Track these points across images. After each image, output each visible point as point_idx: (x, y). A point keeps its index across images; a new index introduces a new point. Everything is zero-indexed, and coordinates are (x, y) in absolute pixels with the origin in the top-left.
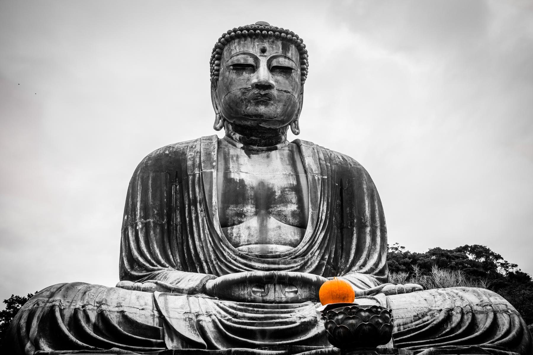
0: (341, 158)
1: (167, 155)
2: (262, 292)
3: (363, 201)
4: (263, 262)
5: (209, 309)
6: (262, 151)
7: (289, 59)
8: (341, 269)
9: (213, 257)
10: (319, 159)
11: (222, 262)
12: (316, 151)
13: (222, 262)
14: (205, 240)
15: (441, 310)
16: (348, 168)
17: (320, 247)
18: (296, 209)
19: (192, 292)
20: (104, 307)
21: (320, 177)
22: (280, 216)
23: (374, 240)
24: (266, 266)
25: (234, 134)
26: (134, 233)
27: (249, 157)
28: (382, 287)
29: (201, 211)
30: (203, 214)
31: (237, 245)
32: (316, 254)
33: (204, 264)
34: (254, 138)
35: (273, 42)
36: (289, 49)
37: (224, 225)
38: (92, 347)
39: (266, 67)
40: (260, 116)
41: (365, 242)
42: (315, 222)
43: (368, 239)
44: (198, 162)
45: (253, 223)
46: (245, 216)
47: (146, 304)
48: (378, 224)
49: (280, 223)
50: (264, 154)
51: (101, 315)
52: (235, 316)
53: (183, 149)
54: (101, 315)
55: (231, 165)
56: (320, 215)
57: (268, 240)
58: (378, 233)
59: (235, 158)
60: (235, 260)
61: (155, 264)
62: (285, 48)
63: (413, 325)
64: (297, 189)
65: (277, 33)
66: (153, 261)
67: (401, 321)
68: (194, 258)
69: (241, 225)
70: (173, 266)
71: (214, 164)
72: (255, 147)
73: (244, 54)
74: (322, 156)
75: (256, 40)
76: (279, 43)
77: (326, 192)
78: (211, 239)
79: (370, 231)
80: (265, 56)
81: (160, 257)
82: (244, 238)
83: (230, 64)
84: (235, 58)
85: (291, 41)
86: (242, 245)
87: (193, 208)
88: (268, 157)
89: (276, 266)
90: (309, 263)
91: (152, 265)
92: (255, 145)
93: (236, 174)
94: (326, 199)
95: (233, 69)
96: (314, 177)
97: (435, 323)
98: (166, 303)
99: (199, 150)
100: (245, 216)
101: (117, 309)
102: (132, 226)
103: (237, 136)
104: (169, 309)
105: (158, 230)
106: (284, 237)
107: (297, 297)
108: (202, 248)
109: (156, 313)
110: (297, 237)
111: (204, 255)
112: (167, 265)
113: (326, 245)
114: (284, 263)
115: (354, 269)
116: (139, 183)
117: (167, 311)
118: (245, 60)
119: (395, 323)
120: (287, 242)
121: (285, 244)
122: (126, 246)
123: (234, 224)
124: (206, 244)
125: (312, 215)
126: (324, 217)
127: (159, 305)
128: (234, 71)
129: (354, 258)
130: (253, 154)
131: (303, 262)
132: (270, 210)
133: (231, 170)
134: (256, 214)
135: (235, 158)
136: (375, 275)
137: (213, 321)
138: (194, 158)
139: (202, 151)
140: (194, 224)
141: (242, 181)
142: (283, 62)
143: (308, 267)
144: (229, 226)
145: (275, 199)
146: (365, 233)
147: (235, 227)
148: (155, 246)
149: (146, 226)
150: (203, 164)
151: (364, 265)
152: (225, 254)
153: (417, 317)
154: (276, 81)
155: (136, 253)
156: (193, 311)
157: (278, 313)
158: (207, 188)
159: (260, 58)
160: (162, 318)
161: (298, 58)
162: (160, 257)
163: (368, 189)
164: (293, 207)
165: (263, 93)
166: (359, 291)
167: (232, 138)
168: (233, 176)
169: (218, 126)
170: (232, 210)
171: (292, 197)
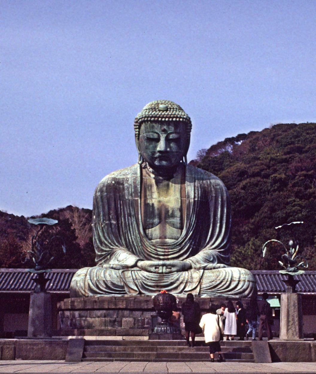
1: (114, 184)
3: (218, 209)
4: (162, 248)
9: (140, 245)
11: (144, 247)
13: (144, 247)
14: (136, 236)
15: (220, 279)
16: (211, 189)
20: (104, 279)
24: (163, 250)
25: (149, 168)
26: (101, 228)
29: (134, 221)
30: (135, 222)
33: (136, 247)
38: (104, 293)
39: (164, 141)
41: (216, 232)
44: (130, 193)
47: (118, 277)
48: (224, 221)
51: (104, 281)
52: (148, 279)
53: (122, 180)
54: (104, 281)
55: (148, 193)
56: (191, 222)
59: (150, 187)
60: (150, 247)
61: (113, 245)
63: (208, 285)
66: (112, 244)
67: (205, 283)
68: (131, 243)
69: (152, 229)
73: (152, 132)
78: (139, 236)
83: (145, 136)
86: (153, 239)
87: (129, 218)
88: (168, 186)
91: (112, 245)
94: (195, 213)
96: (189, 200)
97: (215, 285)
98: (124, 275)
99: (130, 183)
100: (155, 225)
102: (99, 224)
103: (151, 170)
104: (126, 278)
108: (135, 239)
109: (121, 280)
110: (179, 235)
111: (136, 243)
112: (119, 246)
114: (172, 249)
115: (208, 246)
116: (101, 201)
117: (125, 279)
118: (153, 136)
119: (203, 283)
120: (174, 237)
121: (172, 239)
122: (97, 233)
123: (149, 228)
124: (137, 239)
126: (193, 224)
128: (148, 141)
131: (180, 248)
132: (167, 220)
133: (148, 197)
134: (159, 223)
135: (150, 187)
137: (141, 282)
138: (128, 188)
139: (132, 184)
140: (131, 226)
141: (153, 204)
143: (183, 249)
144: (147, 229)
145: (169, 215)
146: (217, 227)
147: (150, 229)
150: (133, 195)
152: (145, 244)
153: (211, 282)
155: (103, 239)
158: (136, 208)
159: (161, 135)
160: (124, 282)
164: (177, 220)
166: (198, 266)
167: (148, 170)
168: (148, 202)
169: (140, 162)
171: (178, 214)
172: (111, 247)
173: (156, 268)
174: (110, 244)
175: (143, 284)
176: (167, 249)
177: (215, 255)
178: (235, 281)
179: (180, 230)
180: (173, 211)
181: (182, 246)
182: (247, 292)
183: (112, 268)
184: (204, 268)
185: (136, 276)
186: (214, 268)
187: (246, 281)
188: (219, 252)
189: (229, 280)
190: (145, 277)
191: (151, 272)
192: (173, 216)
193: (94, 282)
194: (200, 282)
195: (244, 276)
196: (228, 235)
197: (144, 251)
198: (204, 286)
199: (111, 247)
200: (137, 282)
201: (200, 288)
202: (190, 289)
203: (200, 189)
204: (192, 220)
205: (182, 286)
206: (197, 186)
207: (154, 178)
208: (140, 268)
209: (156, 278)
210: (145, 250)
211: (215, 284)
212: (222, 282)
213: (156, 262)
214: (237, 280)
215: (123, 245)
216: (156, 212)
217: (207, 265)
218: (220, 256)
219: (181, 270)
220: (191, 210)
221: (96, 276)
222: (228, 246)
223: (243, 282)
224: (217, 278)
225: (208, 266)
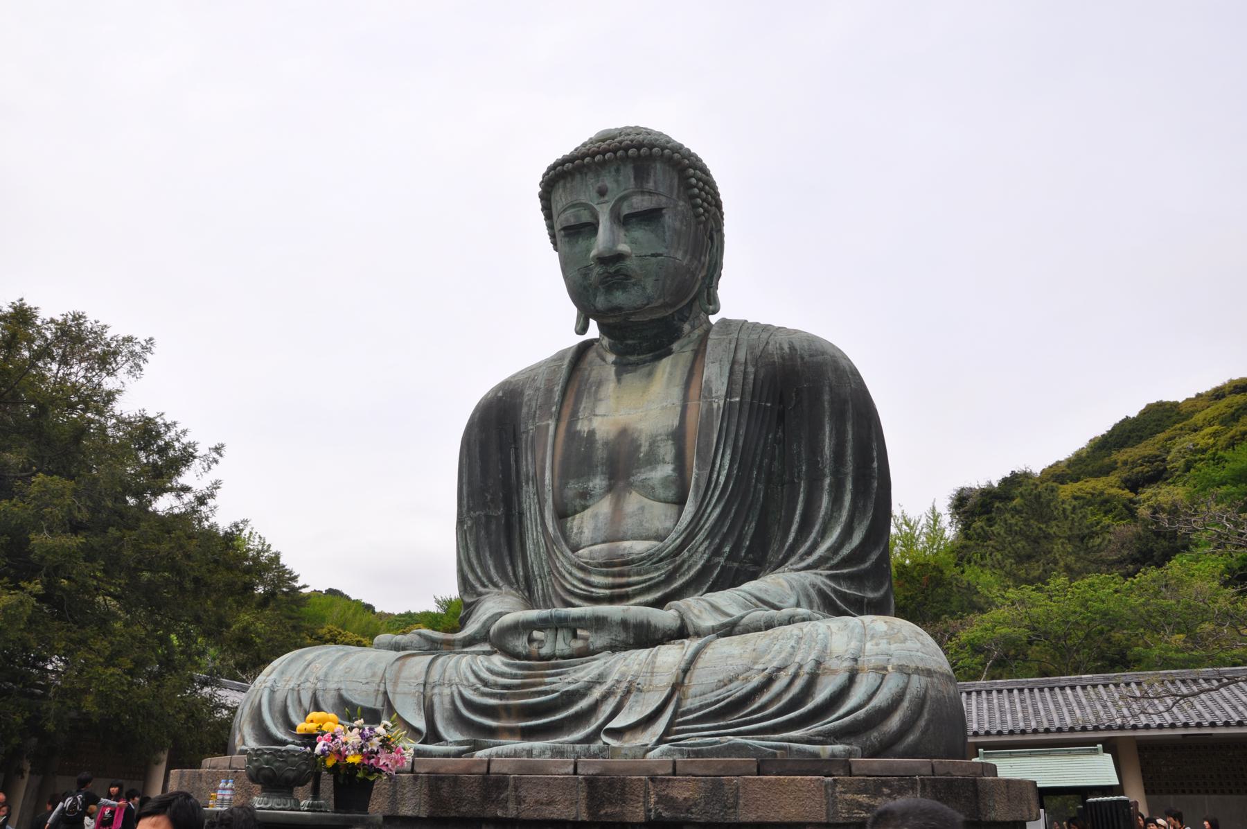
0: (786, 347)
1: (500, 399)
2: (541, 641)
3: (822, 427)
4: (607, 575)
6: (645, 362)
7: (650, 193)
8: (771, 563)
10: (734, 363)
12: (733, 346)
17: (711, 535)
18: (670, 472)
19: (470, 641)
20: (319, 685)
21: (722, 403)
23: (836, 501)
24: (610, 580)
27: (619, 381)
28: (742, 617)
31: (575, 549)
32: (701, 549)
34: (630, 342)
35: (618, 170)
36: (648, 174)
37: (563, 514)
39: (608, 224)
40: (618, 309)
41: (820, 507)
42: (701, 493)
43: (825, 500)
46: (591, 496)
47: (374, 675)
48: (850, 468)
49: (646, 500)
50: (645, 370)
55: (585, 403)
56: (715, 476)
57: (621, 535)
58: (849, 486)
60: (570, 574)
62: (641, 173)
63: (711, 697)
65: (620, 153)
66: (485, 580)
70: (511, 584)
71: (554, 409)
72: (633, 358)
73: (573, 206)
74: (741, 356)
75: (590, 175)
76: (628, 171)
77: (733, 428)
79: (830, 485)
80: (607, 202)
81: (493, 571)
82: (587, 534)
84: (563, 217)
85: (651, 157)
88: (650, 374)
89: (624, 580)
90: (686, 567)
91: (484, 586)
92: (632, 354)
93: (586, 422)
94: (730, 442)
95: (566, 236)
96: (711, 404)
98: (400, 670)
100: (591, 496)
101: (334, 686)
103: (606, 342)
105: (493, 527)
106: (647, 525)
107: (587, 647)
110: (669, 524)
113: (725, 530)
114: (639, 574)
115: (793, 560)
117: (395, 684)
119: (691, 691)
120: (652, 533)
121: (647, 538)
123: (576, 512)
125: (697, 480)
126: (722, 479)
127: (387, 675)
129: (795, 540)
130: (627, 372)
132: (632, 479)
134: (610, 489)
136: (831, 568)
138: (530, 400)
141: (592, 433)
142: (641, 203)
143: (683, 574)
146: (822, 488)
147: (578, 516)
148: (488, 555)
151: (809, 552)
154: (633, 242)
156: (431, 680)
157: (542, 676)
161: (676, 181)
162: (493, 571)
163: (832, 402)
165: (612, 270)
168: (579, 427)
170: (573, 487)
172: (481, 589)
173: (531, 640)
174: (479, 579)
175: (459, 703)
176: (621, 575)
177: (814, 586)
178: (834, 672)
179: (672, 510)
180: (653, 443)
181: (678, 560)
182: (895, 722)
185: (444, 671)
186: (769, 625)
187: (890, 668)
188: (829, 577)
189: (807, 669)
190: (477, 676)
191: (517, 656)
192: (652, 460)
193: (279, 697)
194: (677, 686)
195: (883, 645)
196: (870, 514)
197: (555, 591)
198: (688, 704)
199: (481, 589)
200: (440, 694)
201: (675, 714)
202: (632, 719)
203: (751, 369)
204: (717, 466)
205: (607, 709)
206: (743, 360)
207: (614, 363)
208: (492, 645)
209: (515, 677)
210: (558, 589)
211: (738, 690)
212: (769, 681)
214: (847, 664)
215: (517, 581)
216: (600, 453)
217: (742, 617)
218: (835, 591)
219: (631, 641)
220: (715, 436)
221: (301, 674)
222: (874, 557)
223: (872, 675)
224: (755, 663)
225: (744, 621)
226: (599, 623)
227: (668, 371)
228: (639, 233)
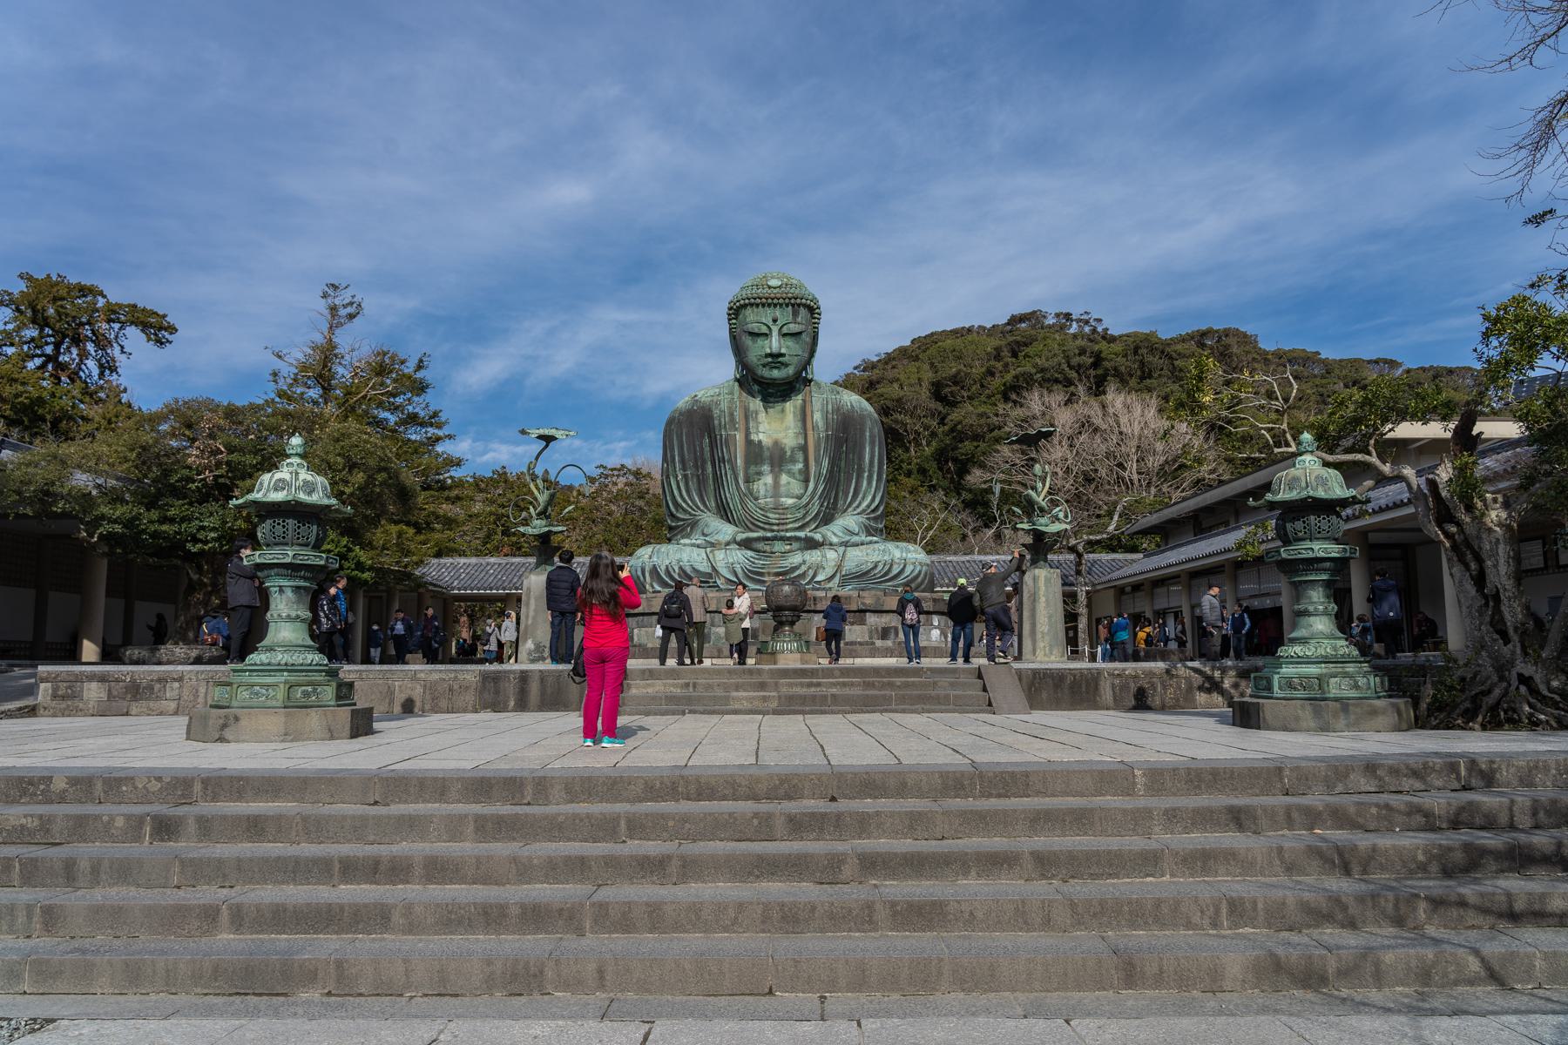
5: (740, 557)
22: (789, 473)
23: (869, 483)
31: (756, 499)
37: (747, 481)
45: (769, 479)
62: (795, 314)
64: (804, 448)
82: (762, 492)
88: (783, 411)
103: (756, 388)
142: (794, 328)
149: (685, 476)
164: (800, 466)
166: (835, 540)
170: (753, 469)
171: (800, 456)
183: (693, 545)
184: (846, 544)
192: (793, 460)
194: (839, 567)
211: (865, 568)
213: (769, 535)
226: (797, 539)
227: (791, 406)
228: (790, 342)
